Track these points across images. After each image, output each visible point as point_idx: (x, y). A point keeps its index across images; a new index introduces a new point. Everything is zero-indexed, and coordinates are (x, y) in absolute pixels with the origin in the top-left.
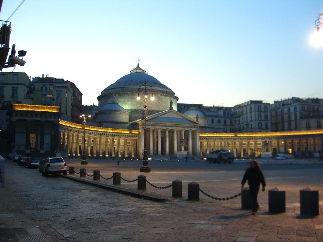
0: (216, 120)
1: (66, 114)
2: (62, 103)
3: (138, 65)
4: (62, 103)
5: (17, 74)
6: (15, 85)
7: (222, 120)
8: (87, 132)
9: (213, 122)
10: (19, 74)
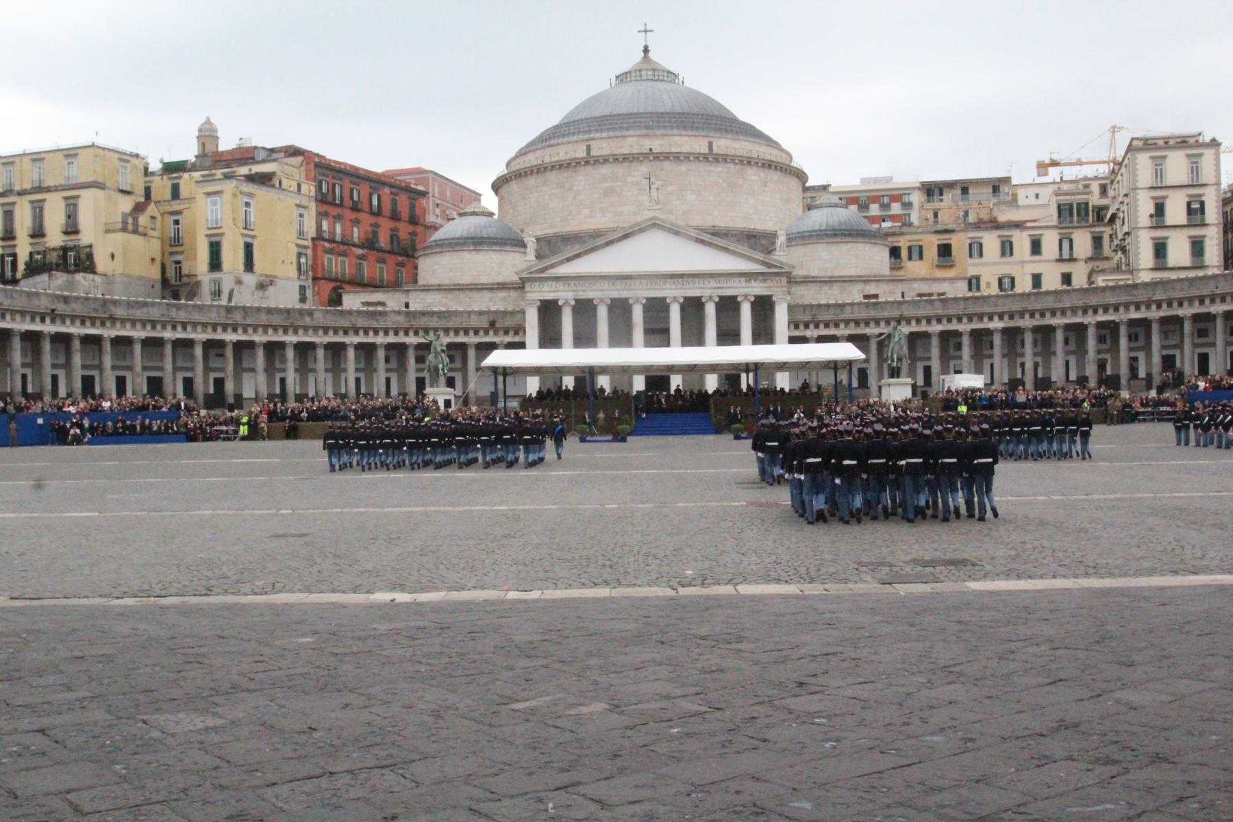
0: (1021, 241)
1: (249, 265)
2: (222, 234)
3: (646, 50)
4: (222, 234)
5: (11, 160)
6: (74, 189)
7: (1050, 242)
8: (204, 331)
9: (1007, 248)
10: (80, 151)
